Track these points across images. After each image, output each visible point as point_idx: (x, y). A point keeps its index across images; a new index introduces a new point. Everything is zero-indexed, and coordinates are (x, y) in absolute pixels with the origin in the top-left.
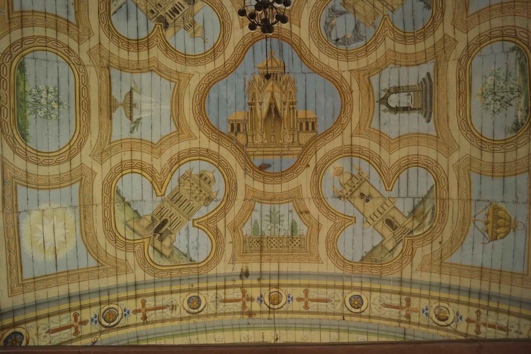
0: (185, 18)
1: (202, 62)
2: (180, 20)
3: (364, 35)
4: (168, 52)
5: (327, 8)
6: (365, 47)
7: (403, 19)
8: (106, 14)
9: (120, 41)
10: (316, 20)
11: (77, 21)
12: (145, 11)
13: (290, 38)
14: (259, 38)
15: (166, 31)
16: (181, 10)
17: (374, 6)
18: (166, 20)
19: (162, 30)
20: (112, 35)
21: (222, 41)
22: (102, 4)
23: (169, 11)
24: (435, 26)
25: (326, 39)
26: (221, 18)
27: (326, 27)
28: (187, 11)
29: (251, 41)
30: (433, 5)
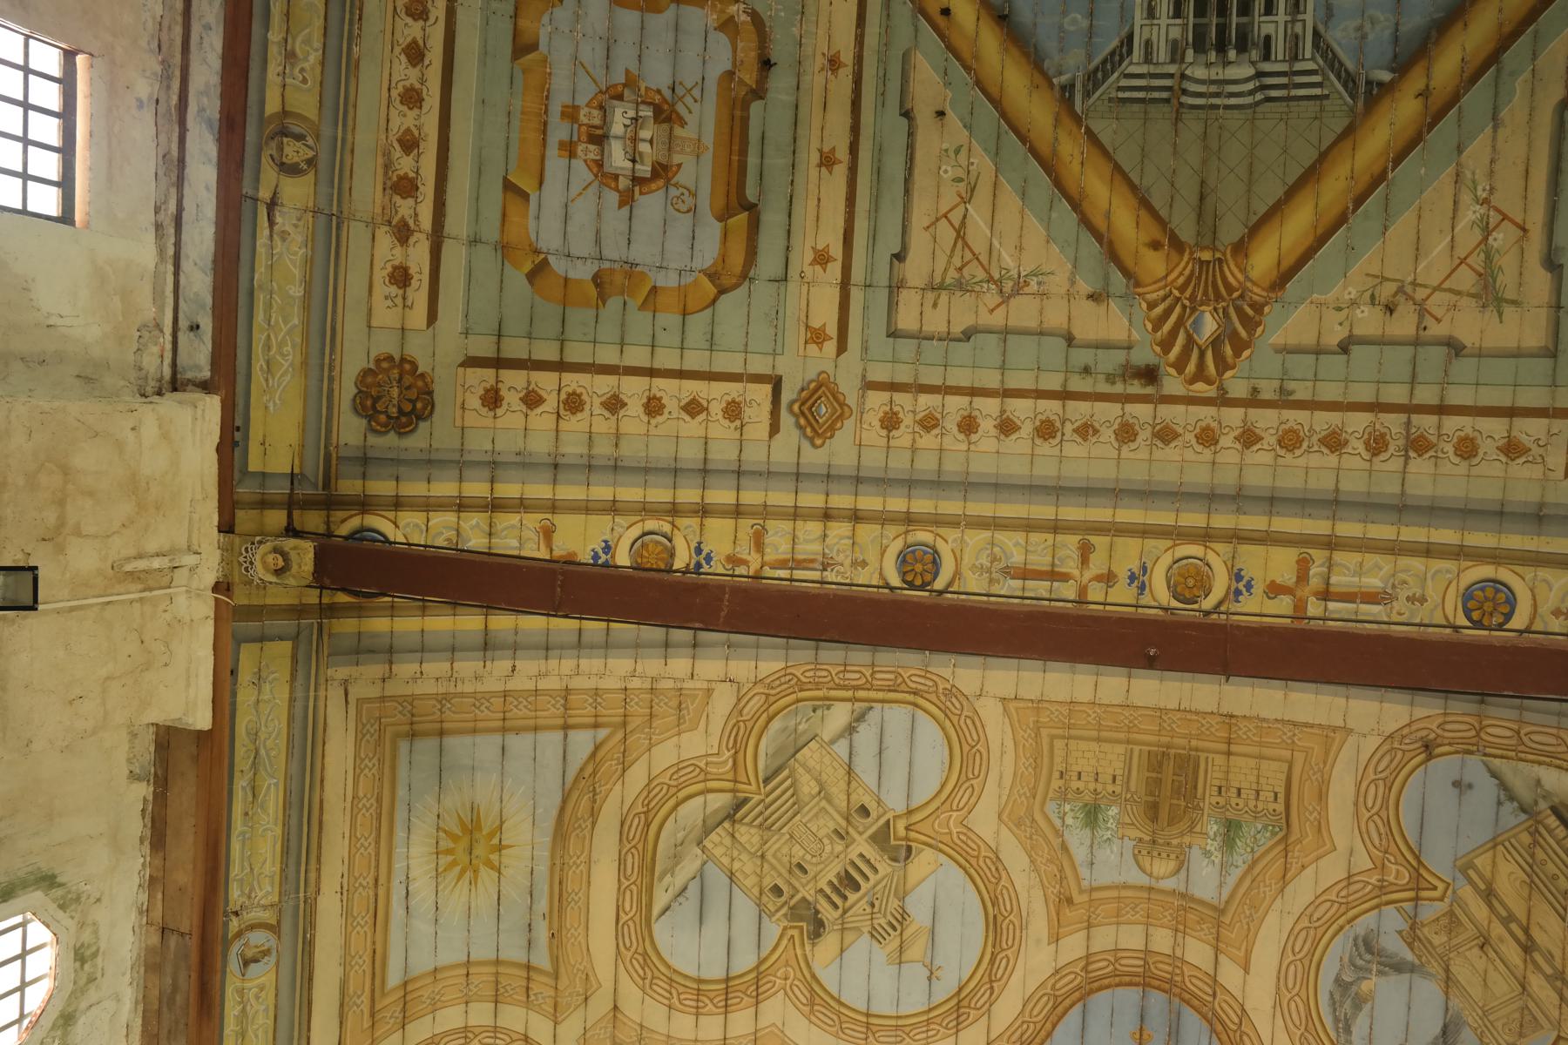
0: (877, 903)
1: (917, 1037)
2: (861, 911)
4: (816, 1008)
8: (638, 922)
9: (674, 991)
10: (1306, 962)
11: (555, 961)
12: (756, 891)
13: (1210, 999)
14: (1106, 982)
15: (814, 945)
16: (867, 878)
18: (817, 912)
19: (803, 945)
20: (653, 978)
21: (986, 979)
22: (628, 893)
23: (830, 883)
25: (1333, 1035)
26: (989, 904)
27: (1337, 997)
29: (1079, 988)
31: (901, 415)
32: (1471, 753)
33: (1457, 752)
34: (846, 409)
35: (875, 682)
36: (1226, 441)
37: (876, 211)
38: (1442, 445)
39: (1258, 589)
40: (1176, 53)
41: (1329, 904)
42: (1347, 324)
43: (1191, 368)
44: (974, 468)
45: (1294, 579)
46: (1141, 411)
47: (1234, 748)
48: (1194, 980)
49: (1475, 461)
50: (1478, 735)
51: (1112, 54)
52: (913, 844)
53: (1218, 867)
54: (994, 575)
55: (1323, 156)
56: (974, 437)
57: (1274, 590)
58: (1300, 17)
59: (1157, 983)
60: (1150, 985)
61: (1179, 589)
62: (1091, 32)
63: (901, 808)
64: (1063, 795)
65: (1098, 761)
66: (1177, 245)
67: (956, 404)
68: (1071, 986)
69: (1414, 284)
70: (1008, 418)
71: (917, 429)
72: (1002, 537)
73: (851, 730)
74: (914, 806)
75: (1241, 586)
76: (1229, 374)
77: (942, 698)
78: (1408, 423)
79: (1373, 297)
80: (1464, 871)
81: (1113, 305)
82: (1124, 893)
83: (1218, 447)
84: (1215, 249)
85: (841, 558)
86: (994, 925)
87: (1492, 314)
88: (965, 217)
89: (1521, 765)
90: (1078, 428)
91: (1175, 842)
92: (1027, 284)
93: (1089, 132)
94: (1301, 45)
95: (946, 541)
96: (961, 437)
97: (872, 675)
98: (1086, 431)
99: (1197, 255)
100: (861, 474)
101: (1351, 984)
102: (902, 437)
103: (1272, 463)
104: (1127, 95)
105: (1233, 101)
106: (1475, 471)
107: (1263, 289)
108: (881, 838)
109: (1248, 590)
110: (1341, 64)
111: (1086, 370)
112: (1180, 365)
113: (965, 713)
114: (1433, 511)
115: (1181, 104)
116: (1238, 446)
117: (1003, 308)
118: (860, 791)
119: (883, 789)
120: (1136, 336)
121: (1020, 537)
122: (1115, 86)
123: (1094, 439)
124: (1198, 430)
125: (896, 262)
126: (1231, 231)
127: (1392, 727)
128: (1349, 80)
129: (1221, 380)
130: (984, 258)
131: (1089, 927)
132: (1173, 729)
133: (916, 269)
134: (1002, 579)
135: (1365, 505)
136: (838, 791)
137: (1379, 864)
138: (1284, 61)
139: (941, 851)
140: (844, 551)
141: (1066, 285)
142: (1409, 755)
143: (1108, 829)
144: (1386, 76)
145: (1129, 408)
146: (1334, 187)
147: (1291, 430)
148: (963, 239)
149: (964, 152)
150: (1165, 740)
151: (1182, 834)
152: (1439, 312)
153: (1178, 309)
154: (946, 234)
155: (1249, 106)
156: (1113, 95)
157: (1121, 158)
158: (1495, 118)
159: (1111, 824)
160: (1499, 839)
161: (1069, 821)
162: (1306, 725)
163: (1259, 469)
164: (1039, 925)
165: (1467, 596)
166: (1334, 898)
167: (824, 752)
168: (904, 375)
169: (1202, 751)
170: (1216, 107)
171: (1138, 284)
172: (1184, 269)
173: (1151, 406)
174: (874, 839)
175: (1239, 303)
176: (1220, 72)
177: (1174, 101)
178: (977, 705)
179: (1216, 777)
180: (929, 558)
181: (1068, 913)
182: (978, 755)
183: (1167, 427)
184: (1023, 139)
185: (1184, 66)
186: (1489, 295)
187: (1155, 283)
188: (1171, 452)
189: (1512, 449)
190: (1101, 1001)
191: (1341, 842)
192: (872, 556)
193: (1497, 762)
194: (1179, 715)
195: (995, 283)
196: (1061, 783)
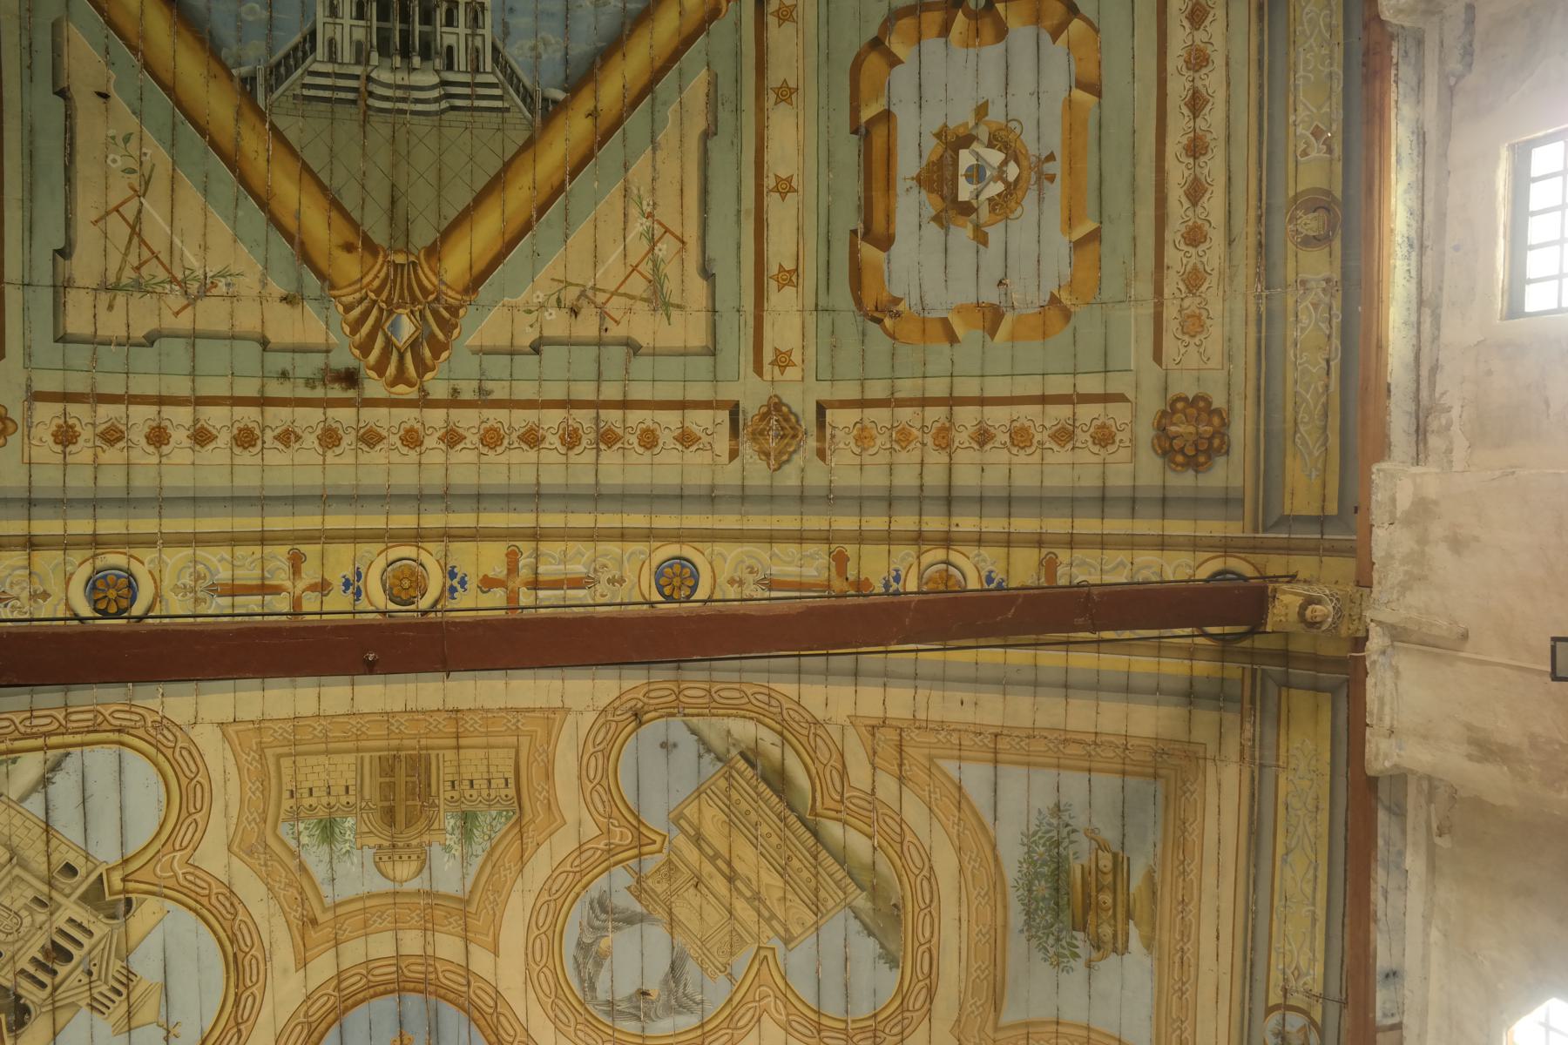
0: (95, 970)
3: (698, 998)
5: (585, 898)
6: (699, 1032)
7: (817, 972)
10: (550, 934)
14: (360, 996)
16: (79, 944)
17: (731, 913)
21: (232, 1023)
24: (906, 1022)
25: (581, 998)
26: (227, 943)
27: (580, 960)
28: (101, 946)
29: (333, 1009)
30: (904, 957)
31: (78, 428)
32: (673, 715)
33: (662, 717)
34: (9, 424)
35: (70, 725)
36: (431, 442)
37: (31, 201)
38: (628, 436)
39: (472, 584)
40: (361, 56)
41: (565, 875)
42: (537, 326)
43: (391, 370)
44: (167, 482)
45: (505, 572)
46: (344, 415)
47: (462, 742)
48: (447, 974)
49: (656, 450)
50: (677, 698)
51: (295, 49)
52: (133, 896)
53: (459, 860)
54: (200, 595)
55: (507, 166)
56: (165, 450)
57: (487, 584)
58: (480, 31)
59: (412, 985)
60: (404, 989)
61: (395, 591)
62: (271, 24)
63: (115, 859)
64: (296, 815)
65: (328, 774)
66: (371, 248)
67: (142, 415)
68: (324, 1009)
69: (594, 288)
70: (202, 427)
71: (98, 443)
72: (203, 553)
73: (45, 782)
74: (130, 853)
75: (455, 582)
76: (429, 376)
77: (153, 732)
78: (598, 418)
79: (559, 301)
80: (676, 822)
81: (309, 307)
82: (369, 903)
83: (423, 448)
84: (408, 252)
85: (15, 591)
86: (235, 964)
87: (660, 316)
88: (140, 212)
89: (714, 719)
90: (279, 435)
91: (414, 843)
92: (214, 285)
93: (273, 128)
94: (481, 58)
95: (142, 563)
96: (151, 449)
97: (66, 717)
98: (288, 437)
99: (392, 258)
100: (33, 496)
101: (591, 944)
102: (82, 452)
103: (476, 460)
104: (312, 93)
105: (420, 107)
106: (657, 459)
107: (457, 292)
108: (94, 897)
109: (462, 587)
110: (519, 80)
111: (284, 375)
112: (380, 368)
113: (180, 744)
114: (624, 498)
115: (368, 107)
116: (443, 446)
117: (189, 311)
118: (63, 848)
119: (91, 843)
120: (333, 339)
121: (225, 552)
122: (299, 82)
123: (297, 446)
124: (402, 432)
125: (60, 259)
126: (423, 235)
127: (603, 702)
128: (527, 96)
129: (421, 382)
130: (164, 257)
131: (336, 945)
132: (401, 731)
133: (85, 265)
134: (208, 597)
135: (564, 496)
136: (35, 855)
137: (605, 830)
138: (467, 72)
139: (166, 897)
140: (18, 583)
141: (257, 287)
142: (621, 725)
143: (346, 841)
144: (560, 95)
145: (331, 412)
146: (519, 196)
147: (492, 429)
148: (139, 235)
149: (134, 141)
150: (394, 743)
151: (421, 834)
152: (616, 315)
153: (375, 312)
154: (119, 230)
155: (436, 113)
156: (298, 92)
157: (307, 156)
158: (653, 141)
159: (349, 836)
160: (702, 789)
161: (305, 839)
162: (528, 710)
163: (465, 467)
164: (284, 954)
165: (659, 573)
166: (569, 869)
167: (13, 812)
168: (78, 384)
169: (432, 748)
170: (404, 112)
171: (333, 287)
172: (379, 272)
173: (353, 411)
174: (84, 899)
175: (435, 305)
176: (406, 77)
177: (361, 103)
178: (193, 734)
179: (448, 772)
180: (123, 582)
181: (313, 935)
182: (198, 786)
183: (371, 430)
184: (202, 131)
185: (369, 68)
186: (659, 300)
187: (350, 285)
188: (377, 456)
189: (686, 439)
190: (357, 1018)
191: (570, 817)
192: (55, 587)
193: (695, 720)
194: (406, 717)
195: (179, 284)
196: (292, 802)
